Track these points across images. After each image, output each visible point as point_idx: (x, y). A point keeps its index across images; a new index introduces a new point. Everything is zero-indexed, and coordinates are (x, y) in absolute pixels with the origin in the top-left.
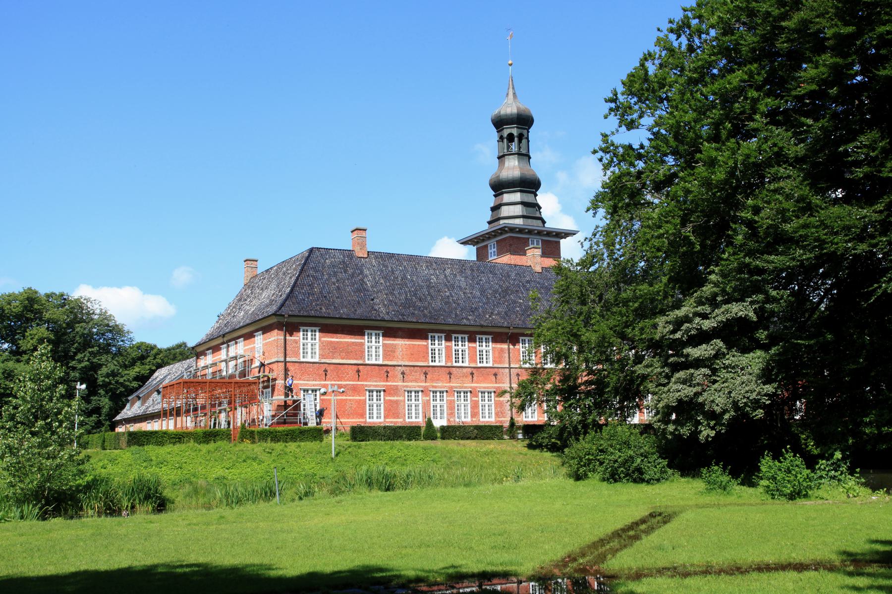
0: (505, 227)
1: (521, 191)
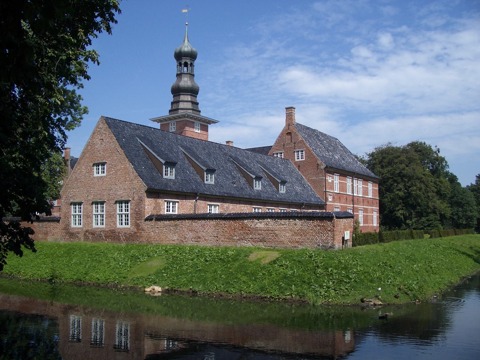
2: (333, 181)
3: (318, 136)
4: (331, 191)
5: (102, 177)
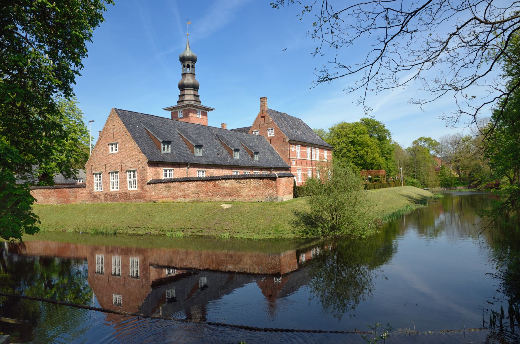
0: (190, 104)
1: (193, 90)
2: (295, 151)
3: (284, 118)
4: (294, 158)
5: (115, 153)
